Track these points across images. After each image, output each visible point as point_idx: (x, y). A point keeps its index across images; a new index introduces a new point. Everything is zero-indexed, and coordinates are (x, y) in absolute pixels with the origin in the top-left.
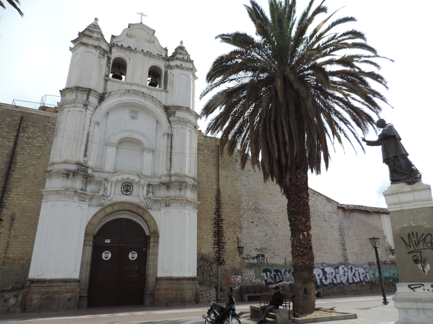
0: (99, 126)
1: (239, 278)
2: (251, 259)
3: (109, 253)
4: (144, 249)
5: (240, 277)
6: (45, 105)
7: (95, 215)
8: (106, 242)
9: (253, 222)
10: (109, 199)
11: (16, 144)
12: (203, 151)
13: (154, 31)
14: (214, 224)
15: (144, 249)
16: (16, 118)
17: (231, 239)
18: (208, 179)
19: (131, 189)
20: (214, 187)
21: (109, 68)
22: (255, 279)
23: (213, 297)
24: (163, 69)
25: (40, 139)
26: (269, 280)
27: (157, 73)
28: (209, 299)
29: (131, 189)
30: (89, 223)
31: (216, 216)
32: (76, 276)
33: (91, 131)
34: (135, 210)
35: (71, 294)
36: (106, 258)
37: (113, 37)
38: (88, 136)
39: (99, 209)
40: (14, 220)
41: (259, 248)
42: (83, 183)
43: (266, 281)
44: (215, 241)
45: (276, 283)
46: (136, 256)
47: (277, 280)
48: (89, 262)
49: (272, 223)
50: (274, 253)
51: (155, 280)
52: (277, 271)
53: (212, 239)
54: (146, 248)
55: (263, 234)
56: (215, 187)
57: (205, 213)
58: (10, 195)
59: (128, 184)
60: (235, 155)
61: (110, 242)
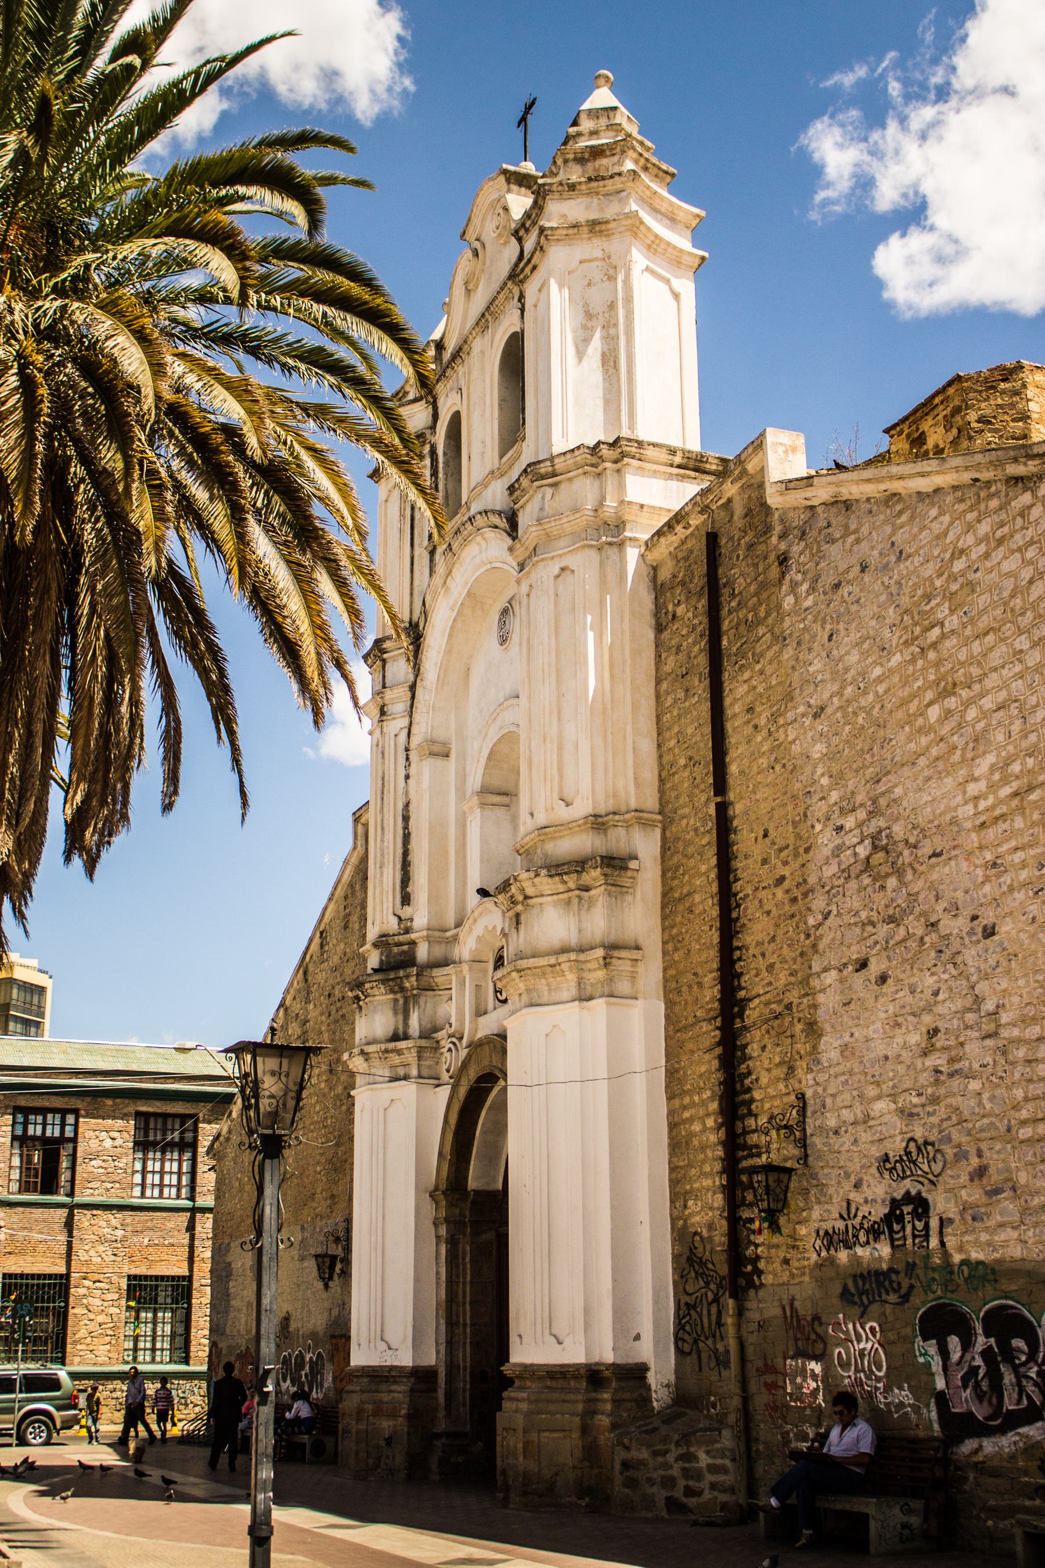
1: (814, 1377)
2: (862, 1238)
5: (816, 1367)
10: (465, 1041)
22: (888, 1389)
23: (713, 1486)
26: (964, 1401)
28: (678, 1493)
32: (405, 1359)
33: (412, 796)
35: (391, 1423)
38: (406, 819)
41: (896, 1147)
42: (395, 1012)
43: (941, 1399)
45: (1002, 1430)
47: (1009, 1405)
50: (981, 1172)
52: (1006, 1324)
55: (915, 1038)
60: (778, 529)
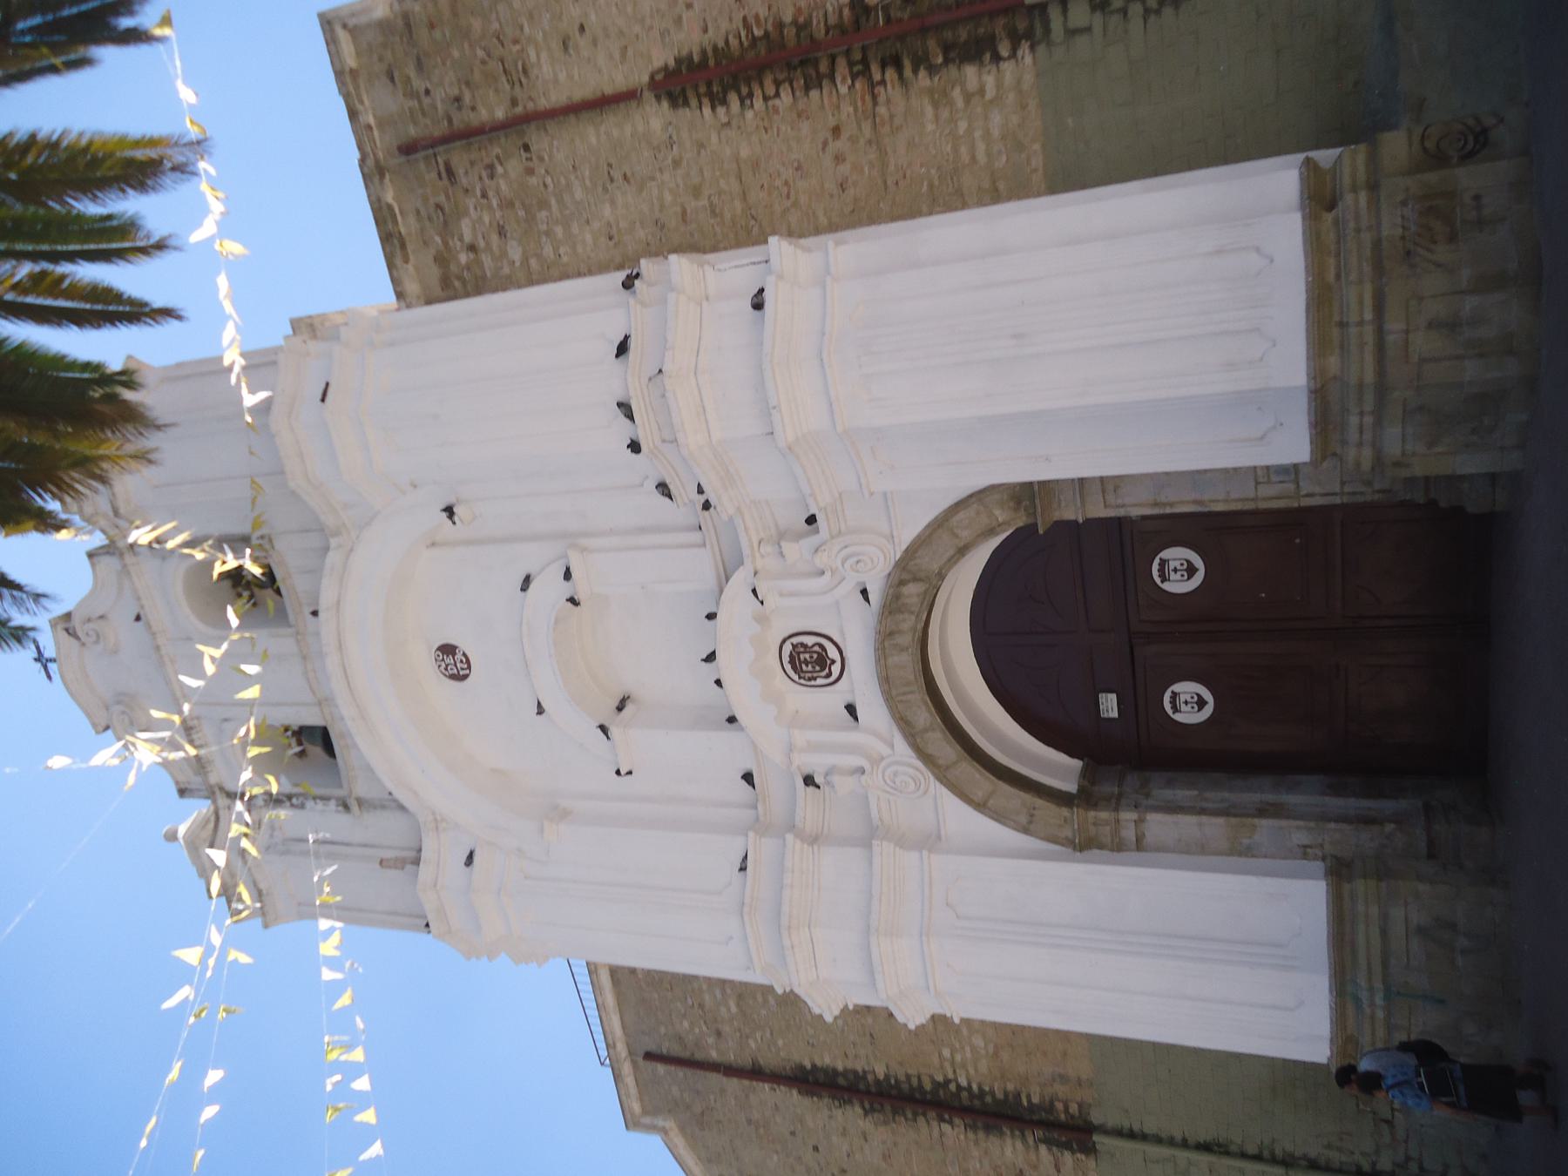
0: (563, 815)
3: (1175, 695)
7: (981, 806)
8: (1115, 714)
10: (885, 750)
11: (755, 1073)
12: (472, 248)
18: (617, 175)
19: (810, 640)
20: (656, 124)
21: (305, 796)
25: (707, 997)
29: (810, 640)
30: (1025, 830)
31: (842, 65)
34: (908, 622)
36: (1201, 703)
37: (182, 792)
39: (945, 791)
40: (1061, 1076)
44: (1015, 40)
46: (1176, 555)
48: (1233, 820)
53: (1008, 67)
56: (655, 117)
57: (839, 159)
58: (959, 1087)
59: (786, 659)
61: (1113, 697)
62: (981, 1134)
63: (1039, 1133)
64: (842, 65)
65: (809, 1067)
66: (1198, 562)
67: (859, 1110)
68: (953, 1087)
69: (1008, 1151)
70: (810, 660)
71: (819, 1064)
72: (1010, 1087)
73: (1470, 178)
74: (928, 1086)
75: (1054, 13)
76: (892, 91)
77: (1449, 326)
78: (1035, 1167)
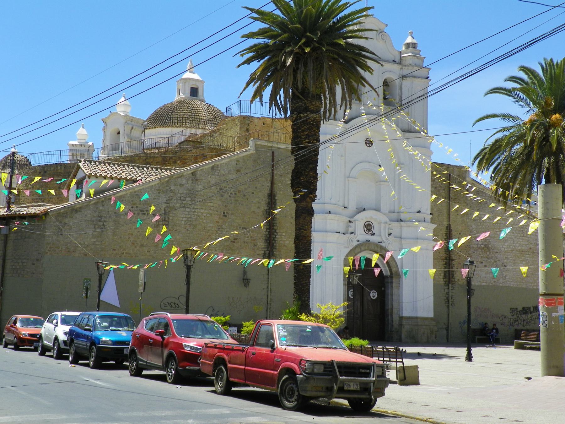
4: (383, 289)
6: (252, 115)
9: (482, 263)
11: (272, 183)
12: (434, 181)
13: (387, 25)
14: (446, 264)
15: (383, 289)
16: (268, 154)
17: (460, 280)
24: (397, 82)
27: (386, 82)
31: (446, 256)
44: (445, 282)
46: (376, 295)
49: (500, 263)
51: (398, 318)
54: (385, 287)
56: (445, 223)
58: (276, 236)
62: (264, 238)
63: (268, 252)
64: (446, 256)
65: (276, 198)
66: (375, 298)
67: (266, 208)
68: (275, 234)
69: (261, 244)
70: (369, 227)
71: (277, 201)
72: (277, 247)
73: (434, 336)
74: (275, 228)
75: (447, 287)
76: (443, 262)
77: (424, 334)
78: (258, 249)
